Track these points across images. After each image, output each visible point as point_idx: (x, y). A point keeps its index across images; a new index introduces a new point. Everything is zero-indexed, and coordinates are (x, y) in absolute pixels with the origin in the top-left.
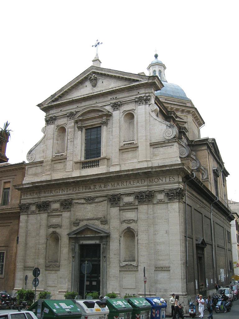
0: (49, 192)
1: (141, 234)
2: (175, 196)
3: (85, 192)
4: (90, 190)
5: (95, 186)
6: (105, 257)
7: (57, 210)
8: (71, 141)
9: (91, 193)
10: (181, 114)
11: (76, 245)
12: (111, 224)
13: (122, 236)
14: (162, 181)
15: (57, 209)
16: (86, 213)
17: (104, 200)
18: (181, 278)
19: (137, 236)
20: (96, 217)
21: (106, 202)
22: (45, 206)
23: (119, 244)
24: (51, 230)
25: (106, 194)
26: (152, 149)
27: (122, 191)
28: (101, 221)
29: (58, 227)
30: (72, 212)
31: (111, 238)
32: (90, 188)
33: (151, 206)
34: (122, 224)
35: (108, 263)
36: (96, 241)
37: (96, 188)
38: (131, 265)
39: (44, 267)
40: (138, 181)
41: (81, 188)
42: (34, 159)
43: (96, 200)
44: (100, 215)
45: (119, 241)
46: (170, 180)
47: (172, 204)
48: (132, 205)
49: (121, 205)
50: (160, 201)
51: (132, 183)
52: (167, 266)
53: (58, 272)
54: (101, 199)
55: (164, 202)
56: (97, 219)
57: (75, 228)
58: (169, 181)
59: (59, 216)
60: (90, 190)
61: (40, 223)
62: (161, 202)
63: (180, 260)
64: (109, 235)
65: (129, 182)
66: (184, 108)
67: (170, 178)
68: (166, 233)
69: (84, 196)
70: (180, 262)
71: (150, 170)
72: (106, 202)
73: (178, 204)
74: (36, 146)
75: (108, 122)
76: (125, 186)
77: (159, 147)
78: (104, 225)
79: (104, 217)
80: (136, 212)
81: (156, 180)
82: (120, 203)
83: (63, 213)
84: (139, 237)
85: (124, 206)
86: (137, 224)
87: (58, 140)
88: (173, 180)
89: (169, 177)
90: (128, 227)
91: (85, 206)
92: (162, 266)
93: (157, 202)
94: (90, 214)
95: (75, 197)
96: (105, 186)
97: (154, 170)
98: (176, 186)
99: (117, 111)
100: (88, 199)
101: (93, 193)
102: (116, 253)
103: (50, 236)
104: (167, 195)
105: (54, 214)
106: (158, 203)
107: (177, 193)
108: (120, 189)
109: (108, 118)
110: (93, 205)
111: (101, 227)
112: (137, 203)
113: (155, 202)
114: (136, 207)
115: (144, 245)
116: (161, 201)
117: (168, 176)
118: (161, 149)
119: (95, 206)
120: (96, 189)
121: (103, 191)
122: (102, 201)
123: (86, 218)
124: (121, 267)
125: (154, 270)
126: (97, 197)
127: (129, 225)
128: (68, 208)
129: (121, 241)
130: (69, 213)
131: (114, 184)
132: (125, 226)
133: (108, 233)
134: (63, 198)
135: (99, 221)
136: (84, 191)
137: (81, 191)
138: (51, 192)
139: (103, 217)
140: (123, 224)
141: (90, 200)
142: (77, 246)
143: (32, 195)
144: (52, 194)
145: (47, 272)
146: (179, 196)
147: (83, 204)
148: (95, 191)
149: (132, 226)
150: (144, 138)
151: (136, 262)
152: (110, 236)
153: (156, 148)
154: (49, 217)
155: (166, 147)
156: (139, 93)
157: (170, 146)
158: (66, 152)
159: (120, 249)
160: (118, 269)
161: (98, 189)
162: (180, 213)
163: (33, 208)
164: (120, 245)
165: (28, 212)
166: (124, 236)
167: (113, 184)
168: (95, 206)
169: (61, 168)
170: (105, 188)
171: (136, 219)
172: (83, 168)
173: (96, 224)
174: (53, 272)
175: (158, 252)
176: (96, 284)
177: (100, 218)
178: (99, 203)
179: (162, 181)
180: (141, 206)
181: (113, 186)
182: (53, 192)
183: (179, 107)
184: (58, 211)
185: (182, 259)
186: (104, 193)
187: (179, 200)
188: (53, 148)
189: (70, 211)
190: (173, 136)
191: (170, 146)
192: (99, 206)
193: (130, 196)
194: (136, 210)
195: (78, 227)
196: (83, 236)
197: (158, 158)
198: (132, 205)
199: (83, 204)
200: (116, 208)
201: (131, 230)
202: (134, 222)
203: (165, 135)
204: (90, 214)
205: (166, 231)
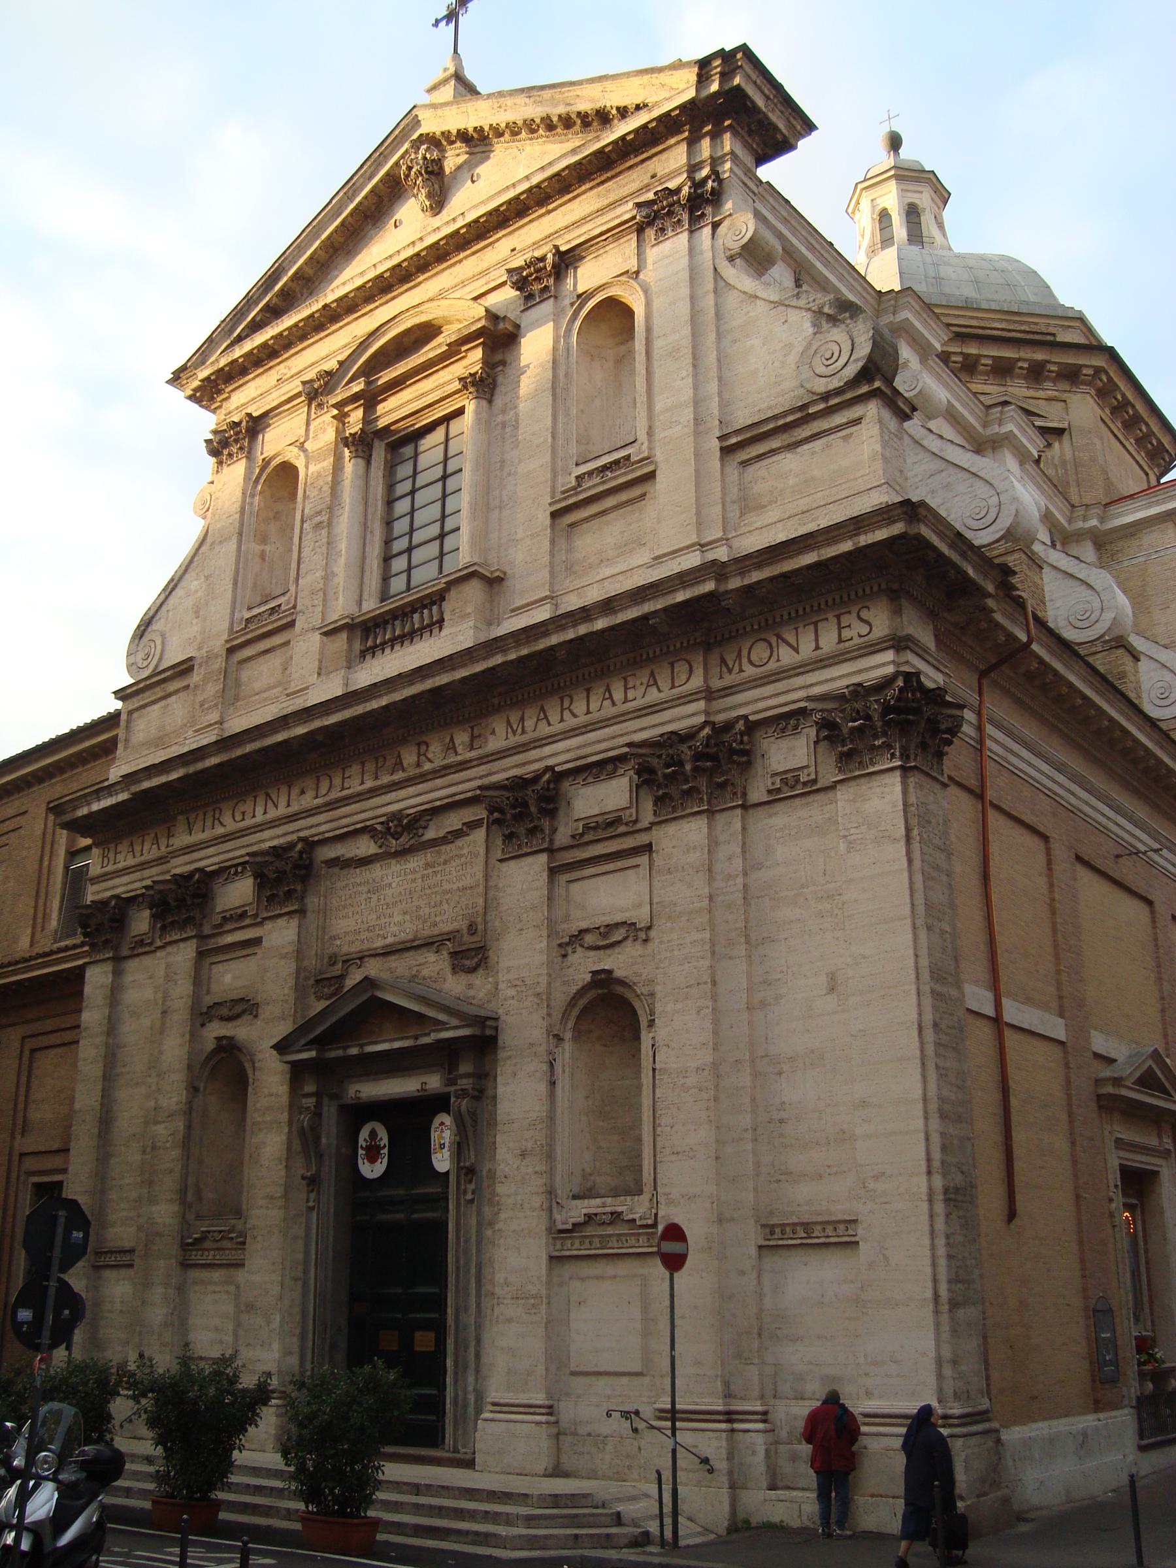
0: (209, 823)
1: (670, 1007)
2: (876, 737)
3: (373, 792)
4: (399, 776)
5: (423, 748)
7: (243, 915)
8: (318, 526)
9: (402, 793)
10: (1031, 393)
11: (325, 1109)
13: (568, 1035)
14: (797, 651)
15: (239, 911)
16: (379, 918)
17: (473, 825)
18: (929, 1294)
19: (651, 1023)
20: (427, 933)
21: (480, 835)
22: (184, 900)
23: (543, 1087)
24: (216, 1030)
25: (479, 783)
26: (733, 471)
27: (560, 754)
28: (454, 955)
29: (244, 1012)
30: (310, 915)
31: (502, 1055)
32: (399, 765)
33: (735, 820)
34: (565, 956)
35: (487, 1210)
36: (423, 1079)
37: (430, 756)
38: (616, 1217)
40: (652, 674)
41: (355, 769)
42: (154, 662)
43: (430, 834)
44: (449, 919)
45: (545, 1067)
46: (846, 634)
47: (864, 786)
48: (622, 829)
49: (563, 836)
50: (784, 781)
51: (618, 695)
52: (840, 1217)
53: (241, 1276)
54: (454, 821)
55: (815, 781)
56: (430, 944)
58: (840, 641)
60: (399, 776)
62: (793, 787)
63: (924, 1169)
64: (488, 1032)
65: (602, 690)
66: (1039, 356)
67: (845, 621)
68: (832, 989)
70: (920, 1184)
71: (709, 586)
72: (480, 835)
73: (898, 788)
74: (171, 588)
75: (500, 379)
76: (583, 719)
77: (773, 452)
78: (471, 978)
79: (472, 929)
80: (644, 871)
81: (760, 652)
82: (554, 830)
83: (269, 925)
84: (662, 1032)
85: (578, 841)
87: (264, 540)
88: (864, 629)
89: (838, 617)
90: (594, 973)
91: (377, 871)
92: (807, 1218)
93: (770, 792)
94: (397, 918)
95: (323, 828)
96: (473, 738)
97: (735, 583)
98: (881, 665)
100: (389, 828)
101: (411, 790)
102: (529, 1145)
104: (829, 731)
105: (229, 939)
106: (775, 798)
107: (887, 709)
108: (552, 739)
109: (499, 357)
110: (415, 863)
111: (454, 986)
112: (648, 817)
113: (757, 794)
114: (643, 839)
115: (690, 1081)
116: (791, 782)
117: (830, 616)
118: (789, 462)
119: (428, 865)
120: (427, 766)
121: (463, 766)
122: (458, 834)
123: (379, 943)
124: (560, 1234)
125: (753, 1251)
126: (435, 812)
127: (607, 961)
128: (289, 895)
130: (294, 923)
131: (522, 719)
133: (481, 1021)
134: (270, 839)
135: (445, 954)
136: (369, 784)
137: (355, 786)
138: (217, 820)
140: (572, 958)
141: (396, 835)
142: (330, 1112)
143: (137, 848)
144: (220, 830)
146: (904, 728)
147: (365, 862)
148: (422, 778)
149: (620, 962)
150: (688, 414)
151: (645, 1197)
152: (500, 1042)
153: (760, 457)
155: (818, 444)
157: (839, 428)
158: (293, 589)
159: (551, 1118)
161: (438, 763)
162: (916, 846)
163: (141, 922)
164: (552, 1095)
165: (116, 948)
166: (578, 1035)
167: (514, 718)
168: (428, 865)
170: (472, 748)
171: (641, 916)
172: (363, 655)
173: (426, 972)
175: (781, 1121)
176: (395, 1348)
177: (451, 936)
178: (448, 847)
179: (797, 651)
180: (672, 829)
181: (514, 732)
182: (227, 818)
183: (1008, 353)
184: (247, 922)
185: (936, 1164)
186: (465, 784)
187: (905, 756)
188: (235, 583)
189: (302, 912)
190: (851, 371)
191: (839, 428)
192: (445, 863)
193: (612, 775)
194: (643, 860)
196: (354, 1051)
197: (773, 515)
198: (622, 829)
199: (365, 862)
200: (530, 859)
201: (619, 990)
203: (806, 373)
204: (397, 918)
205: (832, 977)
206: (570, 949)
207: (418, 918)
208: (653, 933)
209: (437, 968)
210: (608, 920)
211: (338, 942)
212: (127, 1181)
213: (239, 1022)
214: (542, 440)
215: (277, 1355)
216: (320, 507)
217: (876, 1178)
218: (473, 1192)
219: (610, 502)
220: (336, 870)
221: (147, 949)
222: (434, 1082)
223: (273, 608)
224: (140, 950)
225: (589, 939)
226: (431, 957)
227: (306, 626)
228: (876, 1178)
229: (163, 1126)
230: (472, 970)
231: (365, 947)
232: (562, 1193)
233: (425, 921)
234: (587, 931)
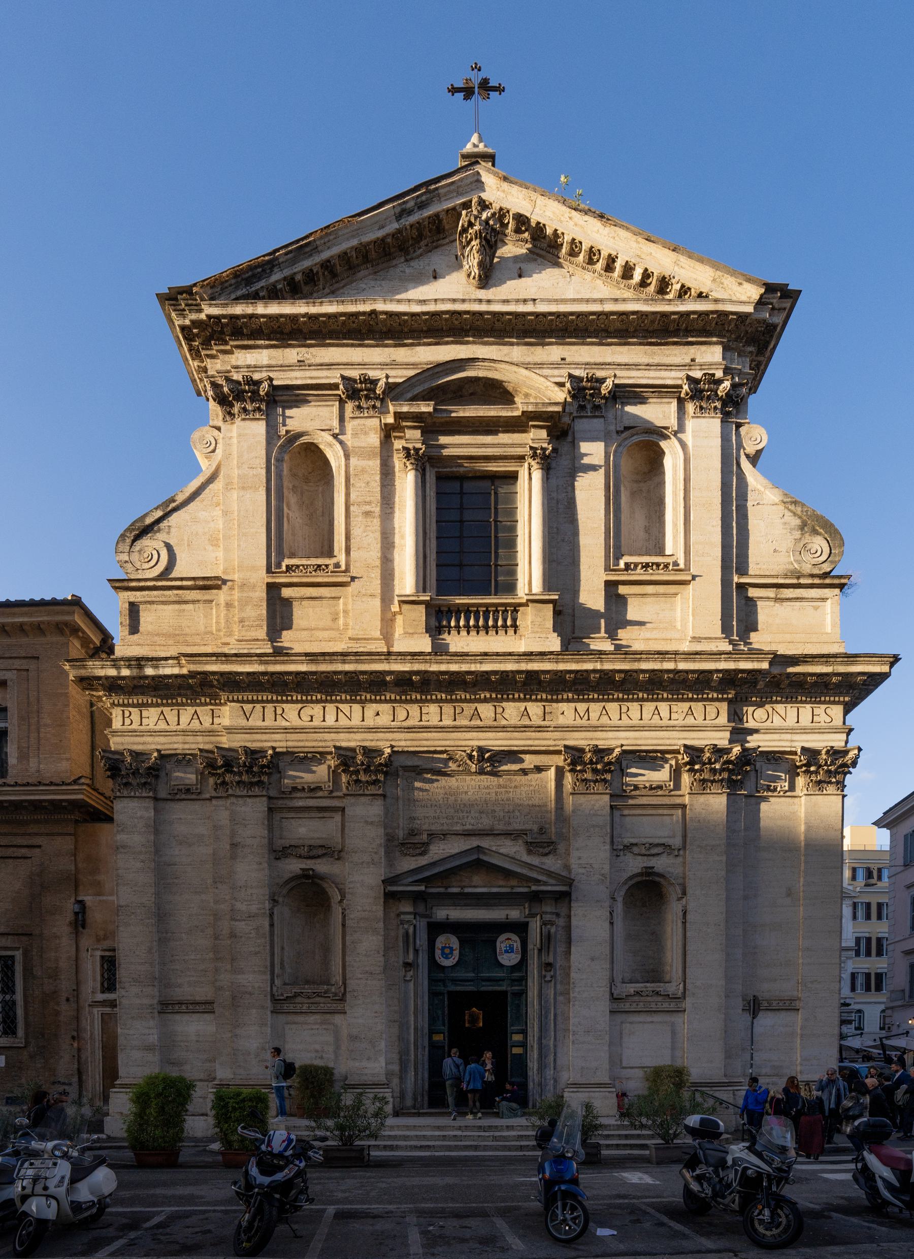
6: (549, 966)
12: (575, 854)
23: (607, 925)
24: (294, 866)
34: (618, 856)
39: (269, 1004)
53: (338, 1019)
57: (408, 864)
59: (326, 814)
61: (233, 834)
69: (447, 743)
86: (680, 859)
99: (595, 420)
103: (288, 887)
123: (458, 828)
129: (615, 914)
132: (634, 865)
135: (520, 841)
139: (535, 828)
140: (622, 858)
142: (422, 924)
145: (282, 1018)
154: (277, 816)
156: (693, 360)
160: (603, 1006)
169: (321, 624)
174: (312, 1018)
195: (423, 861)
202: (669, 854)
206: (622, 853)
207: (495, 817)
208: (681, 852)
209: (514, 850)
210: (651, 841)
211: (419, 822)
212: (193, 957)
213: (319, 861)
214: (595, 526)
215: (384, 1065)
216: (368, 499)
217: (812, 982)
218: (552, 977)
219: (650, 589)
220: (413, 774)
221: (194, 797)
222: (514, 914)
223: (319, 566)
224: (183, 796)
225: (636, 850)
226: (508, 842)
227: (363, 591)
228: (812, 982)
229: (243, 923)
230: (546, 854)
231: (445, 827)
232: (618, 979)
233: (500, 820)
234: (636, 845)
